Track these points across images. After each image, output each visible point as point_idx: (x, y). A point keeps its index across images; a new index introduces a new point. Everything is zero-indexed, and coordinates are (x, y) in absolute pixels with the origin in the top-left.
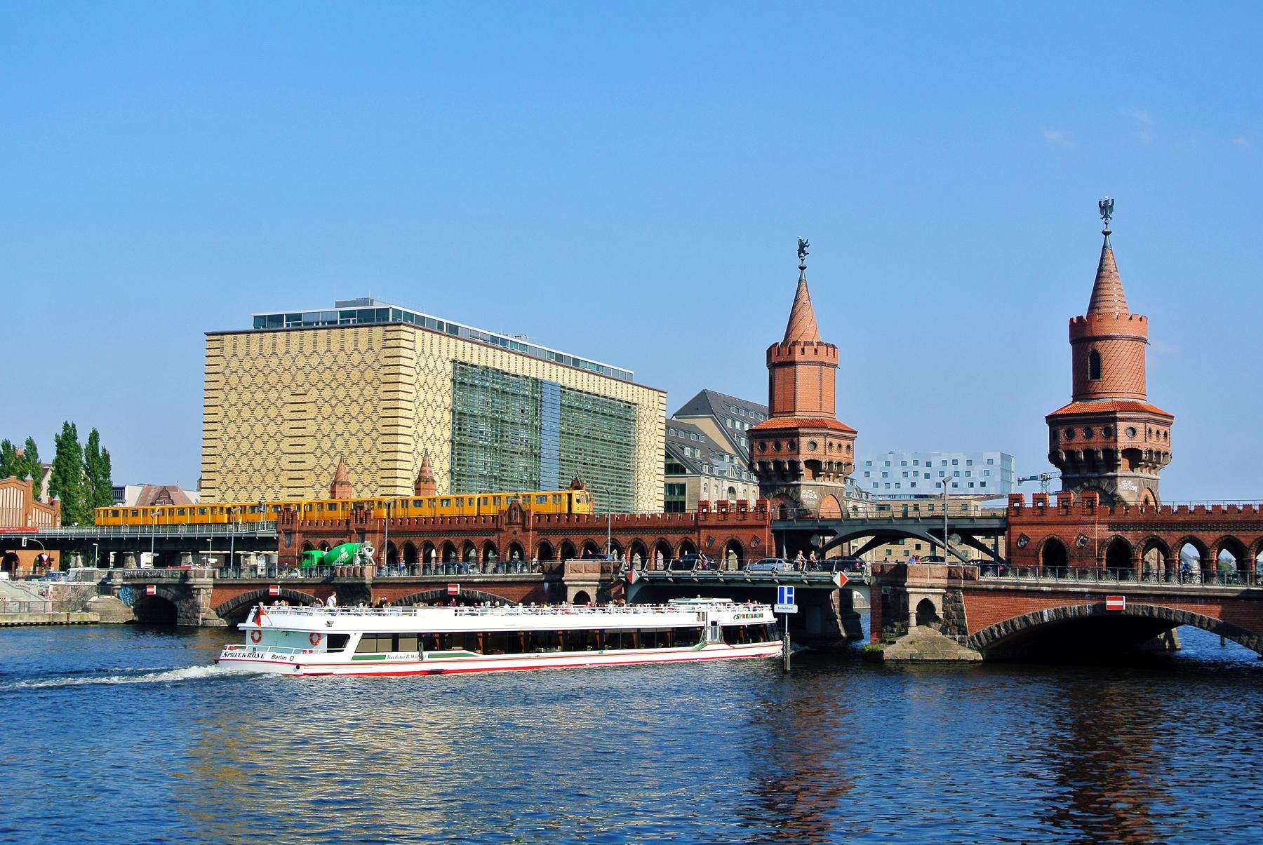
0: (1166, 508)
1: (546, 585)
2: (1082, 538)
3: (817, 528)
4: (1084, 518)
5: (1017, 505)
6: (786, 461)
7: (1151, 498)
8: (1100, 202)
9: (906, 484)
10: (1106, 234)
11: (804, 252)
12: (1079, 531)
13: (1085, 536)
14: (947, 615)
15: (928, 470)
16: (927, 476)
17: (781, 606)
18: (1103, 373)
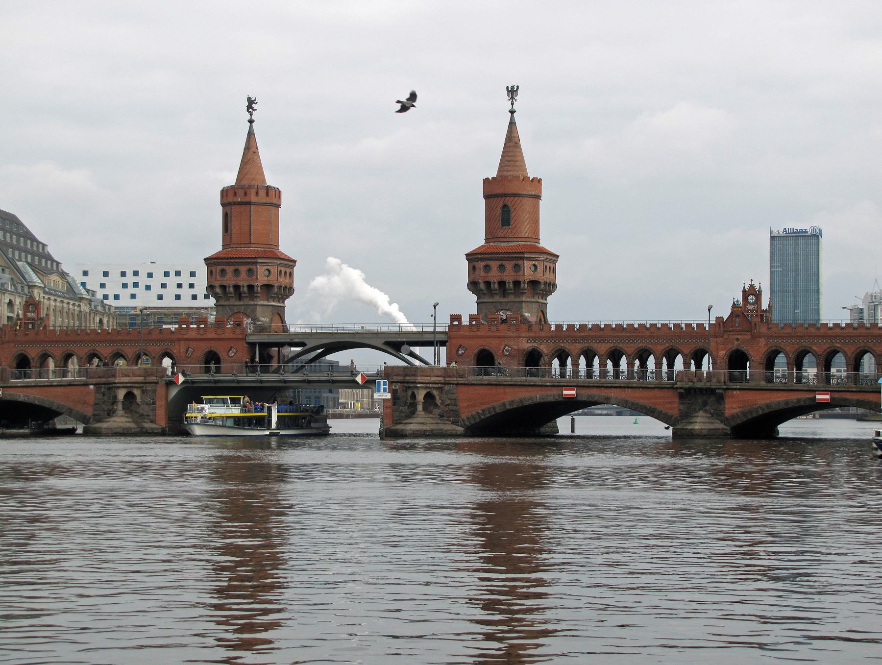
0: (559, 327)
1: (92, 387)
2: (507, 348)
3: (289, 341)
4: (509, 333)
5: (456, 323)
6: (245, 285)
7: (543, 319)
8: (507, 87)
9: (125, 294)
10: (512, 112)
11: (252, 108)
12: (504, 343)
13: (509, 347)
14: (442, 404)
15: (149, 281)
16: (148, 287)
17: (379, 394)
18: (512, 222)
